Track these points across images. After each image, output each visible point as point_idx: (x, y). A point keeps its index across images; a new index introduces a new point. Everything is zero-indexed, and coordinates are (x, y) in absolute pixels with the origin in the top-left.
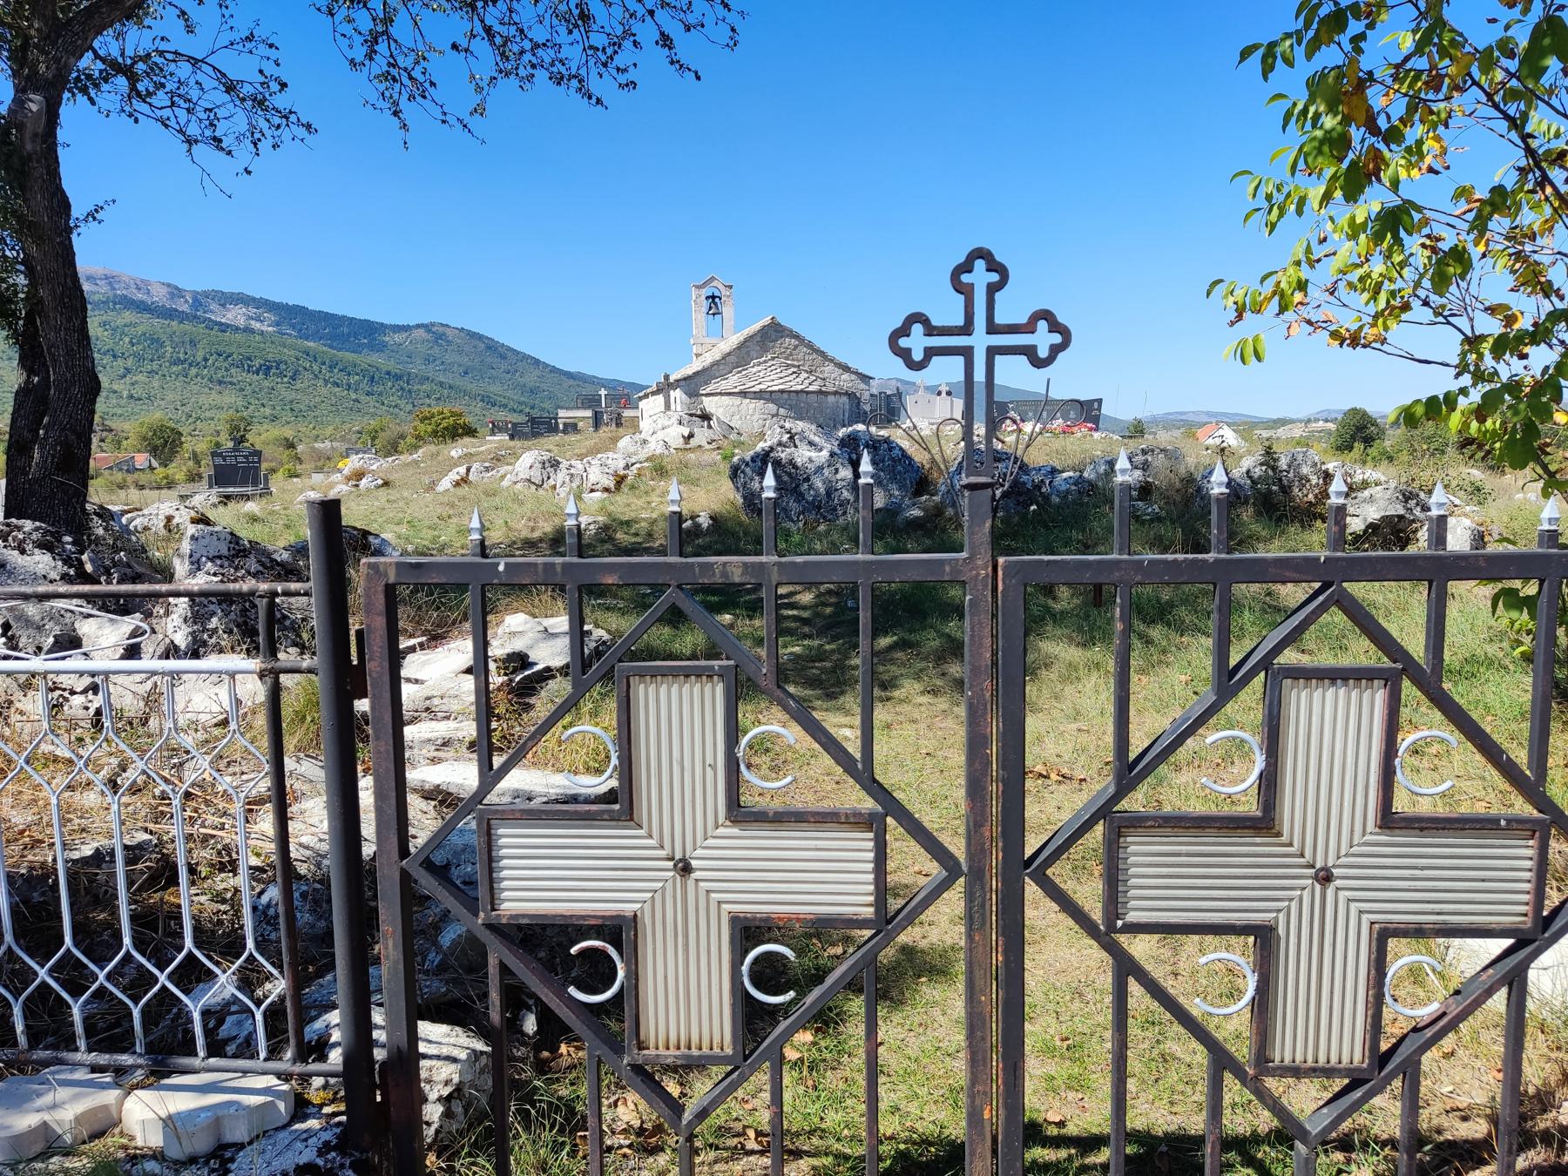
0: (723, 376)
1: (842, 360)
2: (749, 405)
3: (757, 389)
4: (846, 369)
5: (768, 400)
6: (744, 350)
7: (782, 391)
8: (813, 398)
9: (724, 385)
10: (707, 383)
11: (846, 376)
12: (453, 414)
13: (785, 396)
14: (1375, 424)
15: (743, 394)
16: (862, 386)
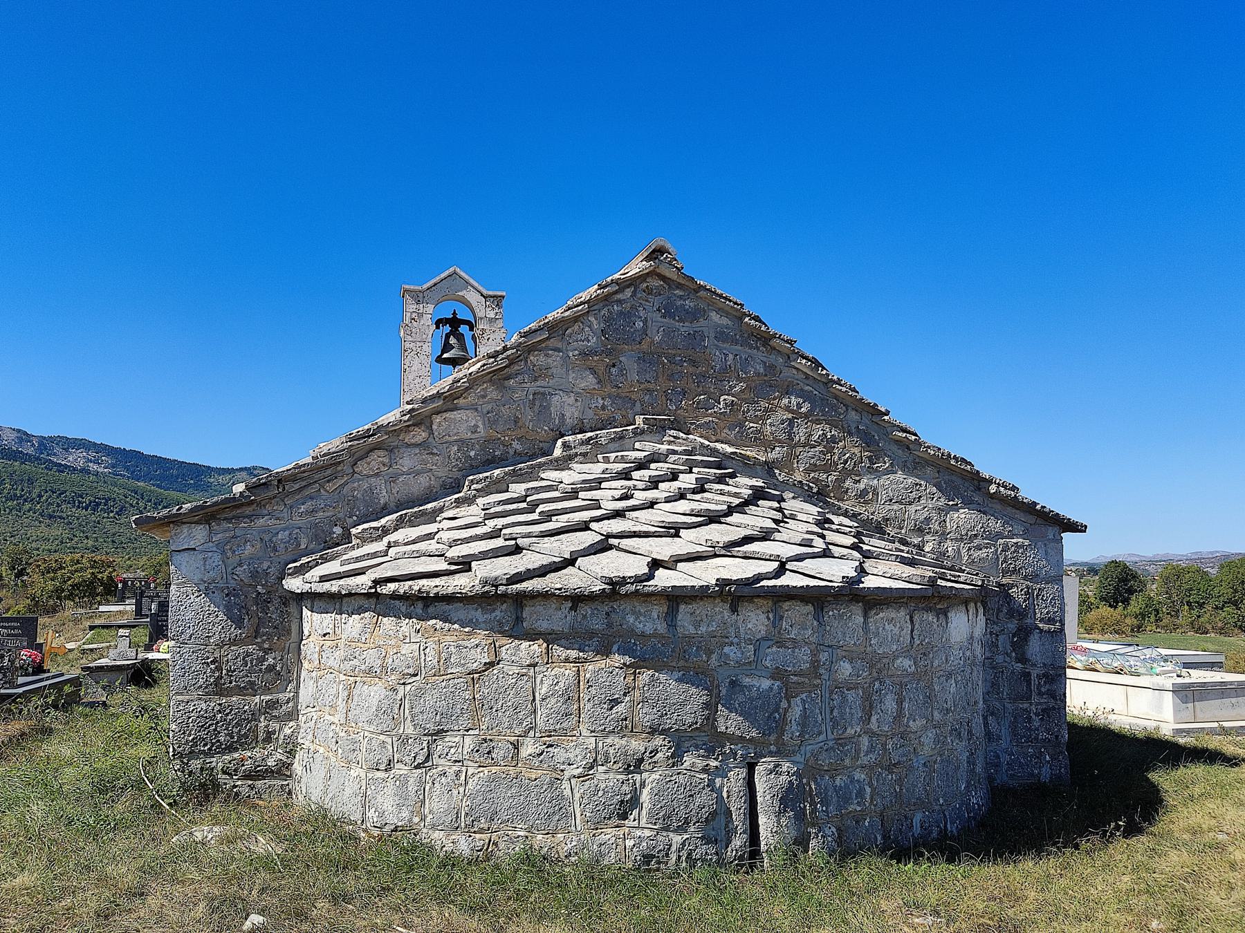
0: (415, 507)
1: (942, 433)
2: (539, 674)
3: (591, 574)
4: (962, 483)
5: (645, 656)
6: (522, 388)
7: (735, 594)
8: (892, 627)
9: (404, 553)
10: (327, 542)
11: (962, 518)
12: (94, 564)
13: (755, 620)
14: (1135, 577)
15: (508, 609)
16: (1032, 559)
